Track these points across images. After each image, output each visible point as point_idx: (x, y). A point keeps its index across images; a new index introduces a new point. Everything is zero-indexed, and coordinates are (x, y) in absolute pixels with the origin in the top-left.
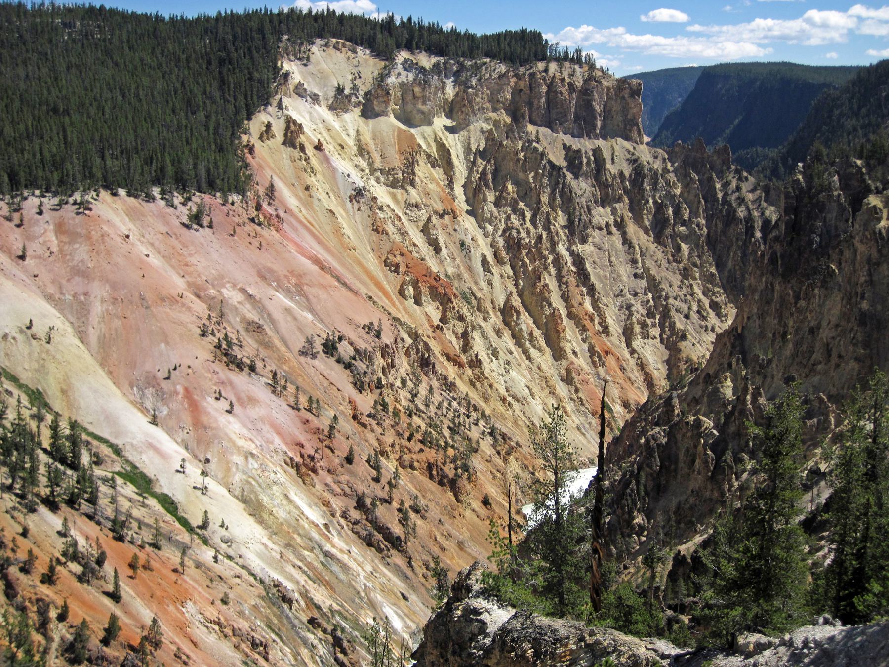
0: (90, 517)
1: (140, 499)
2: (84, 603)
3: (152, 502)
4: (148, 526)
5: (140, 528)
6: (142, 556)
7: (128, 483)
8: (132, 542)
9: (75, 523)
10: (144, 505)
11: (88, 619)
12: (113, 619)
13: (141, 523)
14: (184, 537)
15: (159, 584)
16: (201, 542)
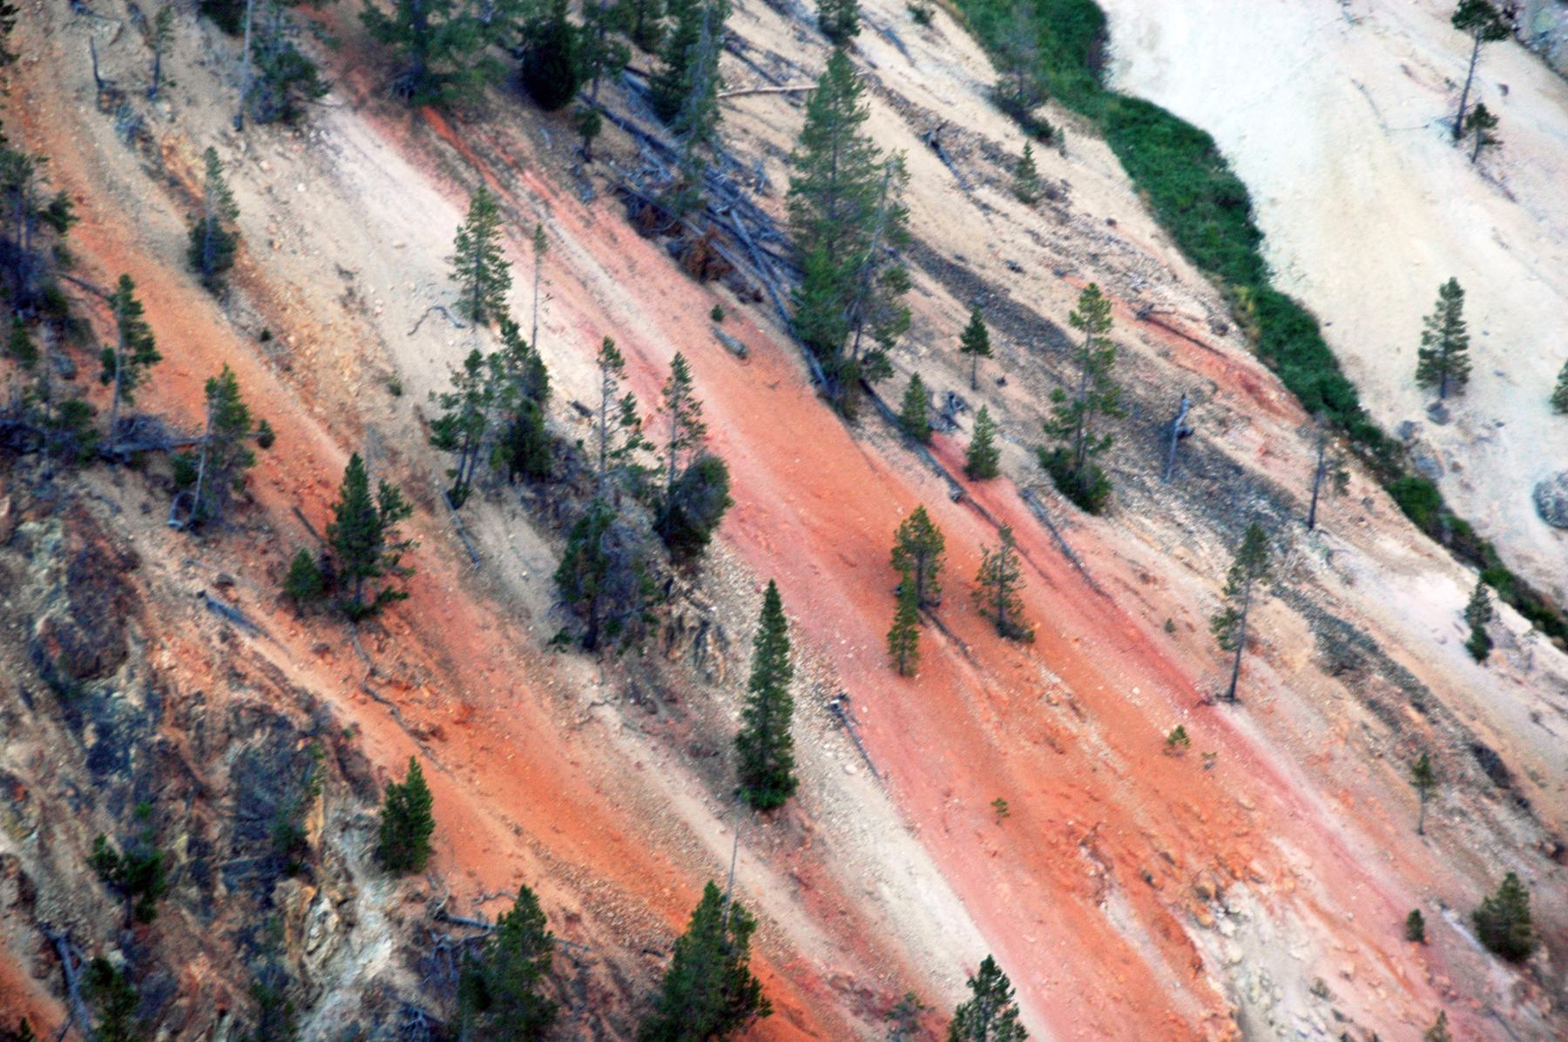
0: (649, 217)
1: (1009, 136)
2: (540, 788)
3: (1091, 172)
4: (1034, 331)
5: (975, 341)
6: (965, 536)
7: (941, 20)
8: (915, 430)
9: (540, 242)
10: (1029, 188)
11: (553, 897)
12: (720, 925)
13: (990, 314)
14: (1271, 443)
15: (1056, 743)
16: (1383, 501)
